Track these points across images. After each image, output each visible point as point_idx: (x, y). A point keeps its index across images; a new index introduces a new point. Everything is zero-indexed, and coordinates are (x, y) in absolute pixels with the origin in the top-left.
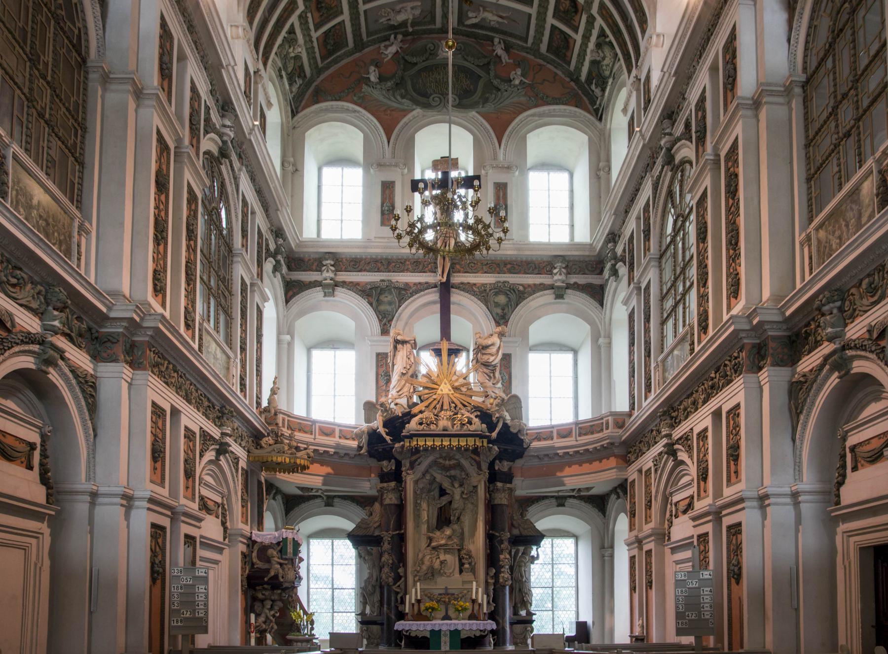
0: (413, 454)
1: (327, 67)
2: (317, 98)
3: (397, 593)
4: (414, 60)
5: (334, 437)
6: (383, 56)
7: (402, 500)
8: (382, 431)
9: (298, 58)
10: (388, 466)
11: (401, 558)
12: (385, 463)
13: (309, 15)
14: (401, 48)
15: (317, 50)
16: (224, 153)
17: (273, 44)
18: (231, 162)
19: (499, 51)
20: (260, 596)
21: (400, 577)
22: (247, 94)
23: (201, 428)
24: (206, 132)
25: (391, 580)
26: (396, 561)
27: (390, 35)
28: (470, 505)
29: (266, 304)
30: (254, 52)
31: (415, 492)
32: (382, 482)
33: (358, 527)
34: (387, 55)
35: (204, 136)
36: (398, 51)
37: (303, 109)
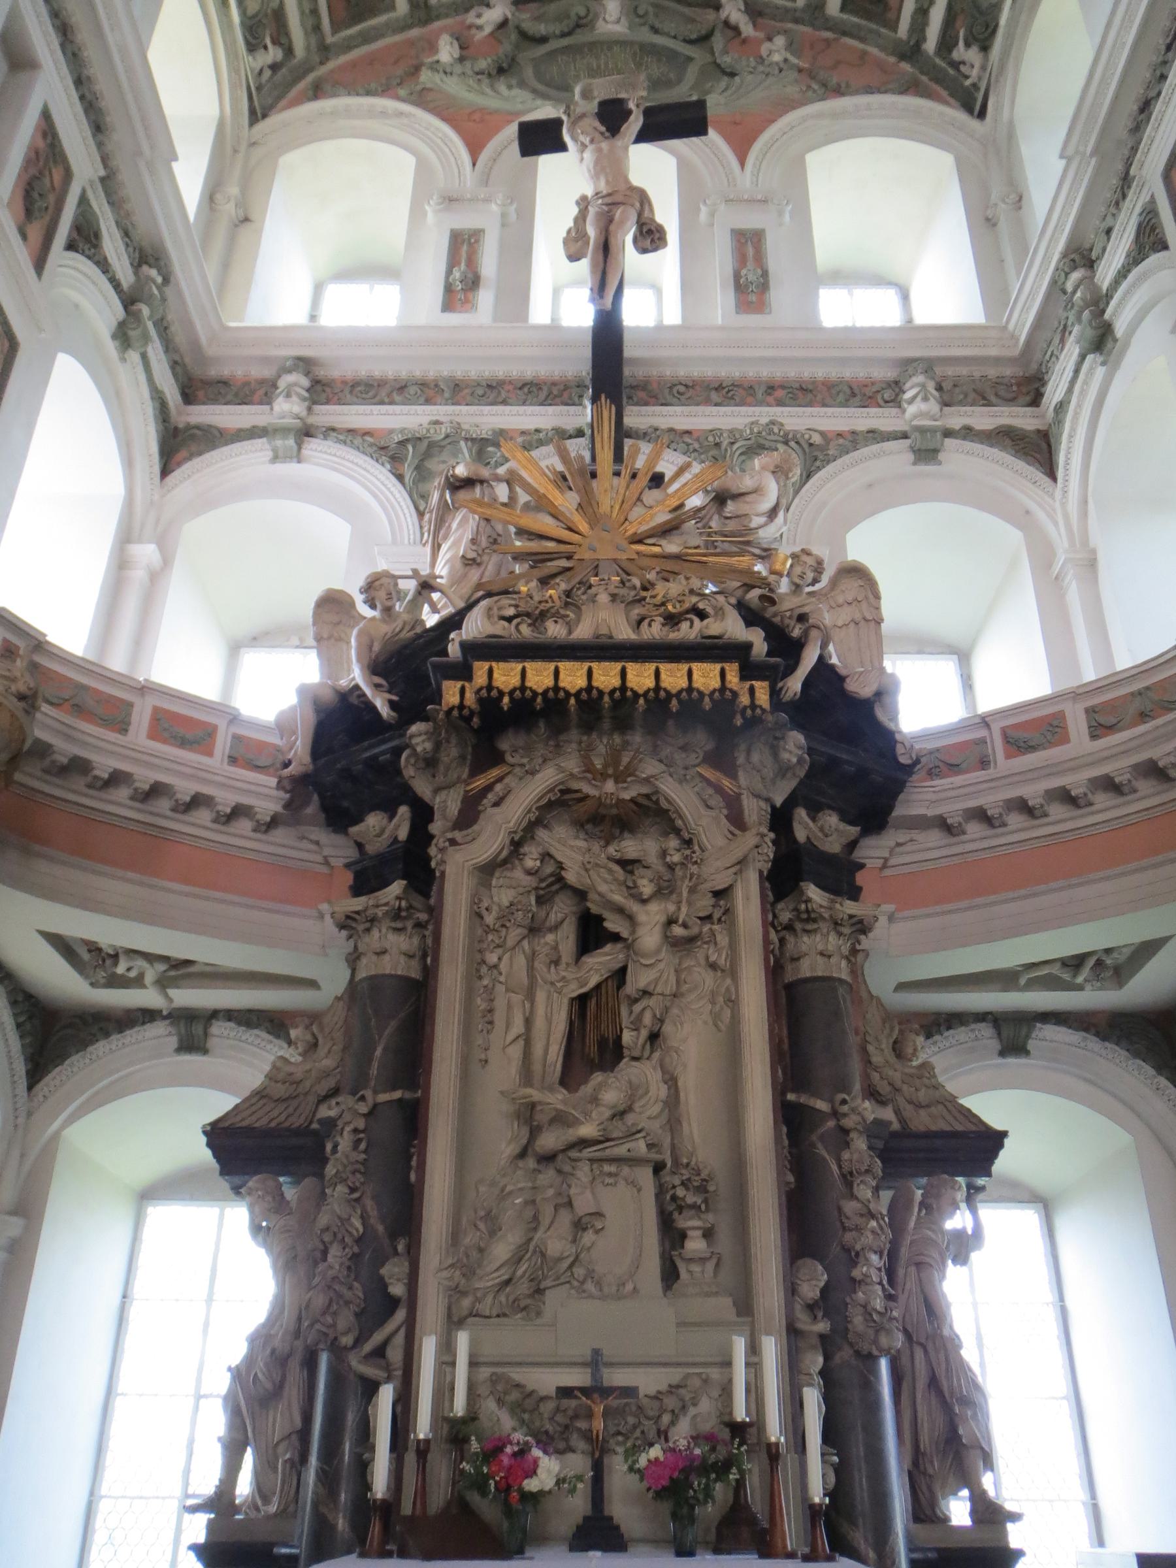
28: (708, 979)
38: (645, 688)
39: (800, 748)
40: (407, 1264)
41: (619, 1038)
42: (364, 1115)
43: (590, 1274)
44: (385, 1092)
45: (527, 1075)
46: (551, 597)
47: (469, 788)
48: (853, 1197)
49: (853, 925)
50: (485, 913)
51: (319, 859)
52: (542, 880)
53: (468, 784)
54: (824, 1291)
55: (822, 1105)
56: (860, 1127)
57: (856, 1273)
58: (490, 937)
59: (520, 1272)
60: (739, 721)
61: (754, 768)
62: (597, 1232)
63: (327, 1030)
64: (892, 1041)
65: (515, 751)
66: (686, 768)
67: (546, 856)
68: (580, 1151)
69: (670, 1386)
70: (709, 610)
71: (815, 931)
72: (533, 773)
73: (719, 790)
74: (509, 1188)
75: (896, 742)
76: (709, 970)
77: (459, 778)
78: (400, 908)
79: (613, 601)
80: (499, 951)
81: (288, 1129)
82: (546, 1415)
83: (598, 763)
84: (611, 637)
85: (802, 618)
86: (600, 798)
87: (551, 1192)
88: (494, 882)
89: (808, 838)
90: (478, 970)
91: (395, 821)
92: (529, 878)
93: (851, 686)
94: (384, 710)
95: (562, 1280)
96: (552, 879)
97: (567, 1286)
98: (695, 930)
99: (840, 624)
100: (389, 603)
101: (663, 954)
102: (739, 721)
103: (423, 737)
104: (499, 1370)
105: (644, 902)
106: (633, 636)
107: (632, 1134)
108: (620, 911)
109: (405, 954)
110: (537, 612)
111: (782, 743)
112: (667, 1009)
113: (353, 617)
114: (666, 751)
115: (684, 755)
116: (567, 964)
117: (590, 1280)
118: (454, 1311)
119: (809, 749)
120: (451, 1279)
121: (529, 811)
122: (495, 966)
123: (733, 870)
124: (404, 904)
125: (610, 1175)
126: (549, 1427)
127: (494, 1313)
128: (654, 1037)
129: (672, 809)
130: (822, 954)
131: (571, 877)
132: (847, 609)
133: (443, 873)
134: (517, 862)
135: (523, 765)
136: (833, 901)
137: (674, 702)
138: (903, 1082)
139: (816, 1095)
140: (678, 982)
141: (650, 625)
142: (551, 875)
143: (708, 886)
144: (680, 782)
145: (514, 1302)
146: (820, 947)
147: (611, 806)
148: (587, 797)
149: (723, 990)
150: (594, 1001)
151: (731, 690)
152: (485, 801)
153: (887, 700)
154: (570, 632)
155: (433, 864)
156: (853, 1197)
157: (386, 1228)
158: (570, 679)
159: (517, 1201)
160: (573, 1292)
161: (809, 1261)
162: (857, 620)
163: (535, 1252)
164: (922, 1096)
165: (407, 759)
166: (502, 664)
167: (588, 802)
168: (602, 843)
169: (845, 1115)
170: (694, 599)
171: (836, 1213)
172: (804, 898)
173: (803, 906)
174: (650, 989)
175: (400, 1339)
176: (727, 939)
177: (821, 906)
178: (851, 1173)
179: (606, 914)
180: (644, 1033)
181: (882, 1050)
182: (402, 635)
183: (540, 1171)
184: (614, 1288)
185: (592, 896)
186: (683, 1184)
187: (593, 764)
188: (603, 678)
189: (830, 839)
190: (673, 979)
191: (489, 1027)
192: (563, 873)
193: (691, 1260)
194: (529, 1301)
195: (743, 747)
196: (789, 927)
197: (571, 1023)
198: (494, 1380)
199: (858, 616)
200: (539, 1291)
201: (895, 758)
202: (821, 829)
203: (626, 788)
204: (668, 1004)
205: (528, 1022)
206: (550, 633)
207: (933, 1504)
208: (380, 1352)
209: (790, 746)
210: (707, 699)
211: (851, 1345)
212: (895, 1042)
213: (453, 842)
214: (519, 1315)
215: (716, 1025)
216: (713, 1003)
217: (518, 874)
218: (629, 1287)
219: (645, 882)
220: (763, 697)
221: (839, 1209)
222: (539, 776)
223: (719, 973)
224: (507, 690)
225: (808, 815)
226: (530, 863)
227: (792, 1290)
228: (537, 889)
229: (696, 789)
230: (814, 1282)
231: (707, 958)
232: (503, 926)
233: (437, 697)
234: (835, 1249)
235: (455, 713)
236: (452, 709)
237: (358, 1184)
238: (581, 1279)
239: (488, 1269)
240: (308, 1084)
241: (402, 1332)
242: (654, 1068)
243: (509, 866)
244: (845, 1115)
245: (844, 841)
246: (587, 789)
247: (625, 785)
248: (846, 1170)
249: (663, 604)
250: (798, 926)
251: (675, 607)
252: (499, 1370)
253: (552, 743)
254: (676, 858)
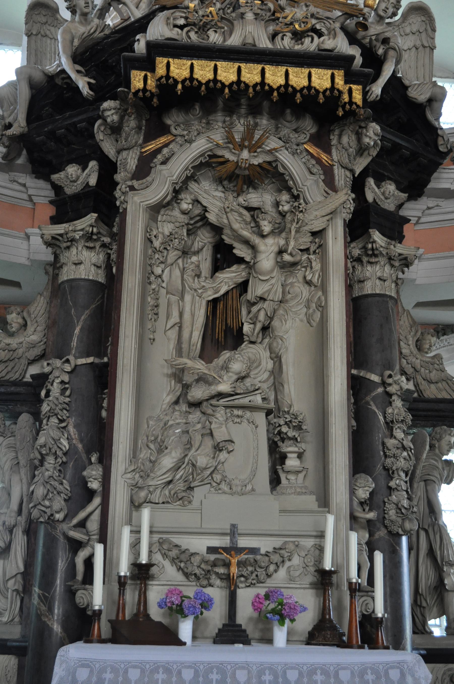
28: (305, 291)
38: (278, 85)
39: (376, 134)
40: (101, 469)
41: (241, 328)
42: (68, 372)
43: (224, 478)
44: (82, 357)
45: (179, 352)
46: (211, 13)
47: (143, 150)
48: (392, 436)
49: (400, 260)
50: (153, 239)
51: (25, 197)
52: (191, 219)
53: (143, 148)
54: (371, 494)
55: (375, 378)
56: (399, 393)
57: (392, 484)
58: (157, 256)
59: (178, 477)
60: (340, 113)
61: (343, 148)
62: (229, 452)
63: (33, 316)
64: (415, 339)
65: (178, 125)
66: (298, 145)
67: (196, 201)
68: (218, 401)
69: (274, 548)
70: (324, 30)
71: (376, 263)
72: (190, 142)
73: (319, 161)
74: (171, 423)
75: (438, 135)
76: (306, 286)
77: (136, 143)
78: (92, 233)
79: (256, 19)
80: (163, 266)
81: (8, 381)
82: (195, 564)
83: (238, 137)
84: (255, 45)
85: (386, 41)
86: (237, 162)
87: (199, 426)
88: (159, 218)
89: (374, 199)
90: (149, 278)
91: (86, 172)
92: (183, 216)
93: (412, 93)
94: (85, 90)
95: (206, 482)
96: (198, 218)
97: (209, 485)
98: (298, 258)
99: (405, 48)
100: (86, 10)
101: (274, 274)
102: (340, 113)
103: (113, 111)
104: (164, 536)
105: (263, 236)
106: (270, 46)
107: (248, 392)
108: (247, 242)
109: (95, 265)
110: (201, 23)
111: (364, 131)
112: (275, 311)
113: (57, 19)
114: (285, 132)
115: (296, 136)
116: (206, 278)
117: (223, 482)
118: (135, 497)
119: (382, 136)
120: (134, 478)
121: (186, 170)
122: (160, 276)
123: (327, 218)
124: (95, 230)
125: (238, 416)
126: (197, 571)
127: (161, 502)
128: (265, 329)
129: (287, 173)
130: (380, 279)
131: (212, 217)
132: (412, 37)
133: (125, 210)
134: (175, 205)
135: (183, 136)
136: (389, 244)
137: (298, 95)
138: (421, 366)
139: (372, 372)
140: (283, 292)
141: (282, 39)
142: (198, 215)
143: (307, 228)
144: (293, 155)
145: (174, 495)
146: (379, 274)
147: (245, 168)
148: (228, 161)
149: (316, 299)
150: (222, 303)
151: (338, 90)
152: (155, 160)
153: (435, 105)
154: (225, 41)
155: (118, 203)
156: (392, 436)
157: (83, 447)
158: (225, 74)
159: (177, 431)
160: (212, 489)
161: (363, 475)
162: (418, 46)
163: (188, 463)
164: (434, 375)
165: (99, 128)
166: (176, 61)
167: (229, 165)
168: (235, 194)
169: (390, 385)
170: (314, 21)
171: (381, 448)
172: (372, 240)
173: (370, 246)
174: (265, 297)
175: (96, 516)
176: (319, 265)
177: (381, 246)
178: (392, 422)
179: (235, 244)
180: (259, 326)
181: (409, 345)
182: (96, 35)
183: (190, 413)
184: (240, 488)
185: (227, 231)
186: (286, 423)
187: (233, 137)
188: (248, 75)
189: (388, 201)
190: (280, 290)
191: (156, 317)
192: (207, 215)
193: (288, 472)
194: (184, 494)
195: (337, 132)
196: (359, 260)
197: (207, 317)
198: (161, 543)
199: (418, 43)
200: (191, 488)
201: (436, 146)
202: (383, 194)
203: (255, 157)
204: (276, 307)
205: (181, 315)
206: (211, 39)
207: (424, 623)
208: (82, 524)
209: (371, 133)
210: (321, 96)
211: (386, 527)
212: (417, 341)
213: (132, 188)
214: (178, 503)
215: (309, 322)
216: (308, 307)
217: (176, 213)
218: (249, 487)
219: (266, 223)
220: (358, 97)
221: (383, 444)
222: (194, 144)
223: (313, 288)
224: (180, 80)
225: (375, 184)
226: (185, 206)
227: (352, 492)
228: (188, 224)
229: (303, 160)
230: (366, 488)
231: (305, 277)
232: (165, 248)
233: (128, 83)
234: (379, 467)
235: (141, 94)
236: (139, 90)
237: (65, 418)
238: (218, 481)
239: (159, 473)
240: (20, 351)
241: (98, 512)
242: (265, 349)
243: (170, 207)
244: (390, 385)
245: (397, 203)
246: (228, 155)
247: (256, 154)
248: (389, 419)
249: (292, 24)
250: (365, 259)
251: (300, 27)
252: (164, 536)
253: (204, 121)
254: (286, 208)
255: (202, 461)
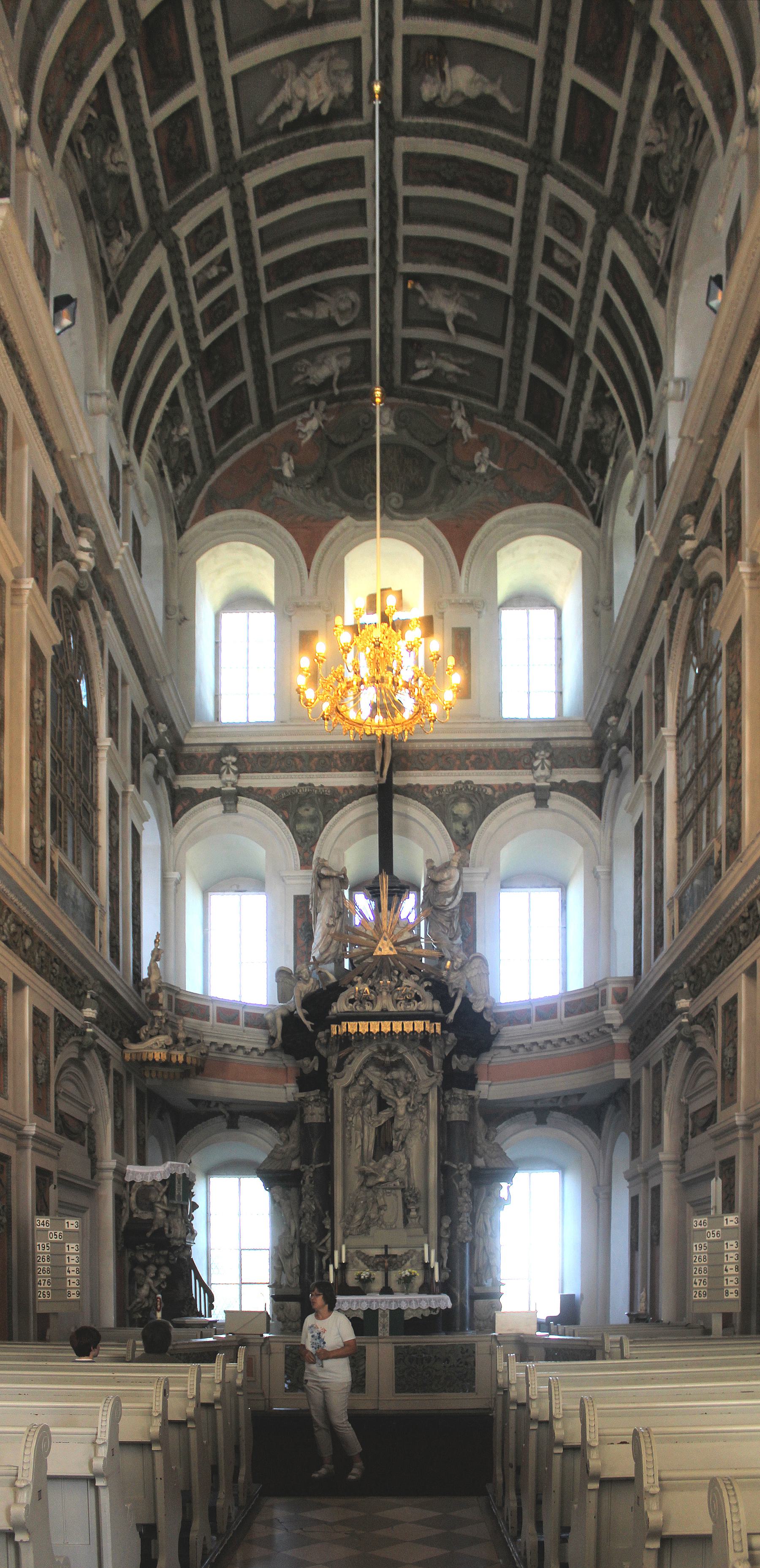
0: (342, 1048)
1: (224, 458)
2: (210, 508)
3: (321, 1255)
4: (343, 440)
5: (238, 1024)
6: (300, 436)
7: (327, 1118)
8: (300, 1013)
9: (184, 445)
10: (311, 1064)
11: (328, 1203)
12: (306, 1061)
13: (198, 375)
14: (324, 422)
15: (209, 430)
16: (82, 595)
17: (149, 422)
18: (91, 604)
19: (459, 422)
20: (141, 1258)
21: (326, 1232)
22: (114, 503)
23: (56, 1010)
24: (56, 560)
25: (313, 1235)
26: (320, 1208)
27: (309, 403)
29: (145, 824)
30: (122, 434)
31: (344, 1105)
32: (301, 1091)
33: (271, 1157)
34: (305, 434)
35: (54, 565)
36: (320, 428)
37: (195, 522)
108: (392, 1100)
226: (361, 1083)
255: (373, 1216)
